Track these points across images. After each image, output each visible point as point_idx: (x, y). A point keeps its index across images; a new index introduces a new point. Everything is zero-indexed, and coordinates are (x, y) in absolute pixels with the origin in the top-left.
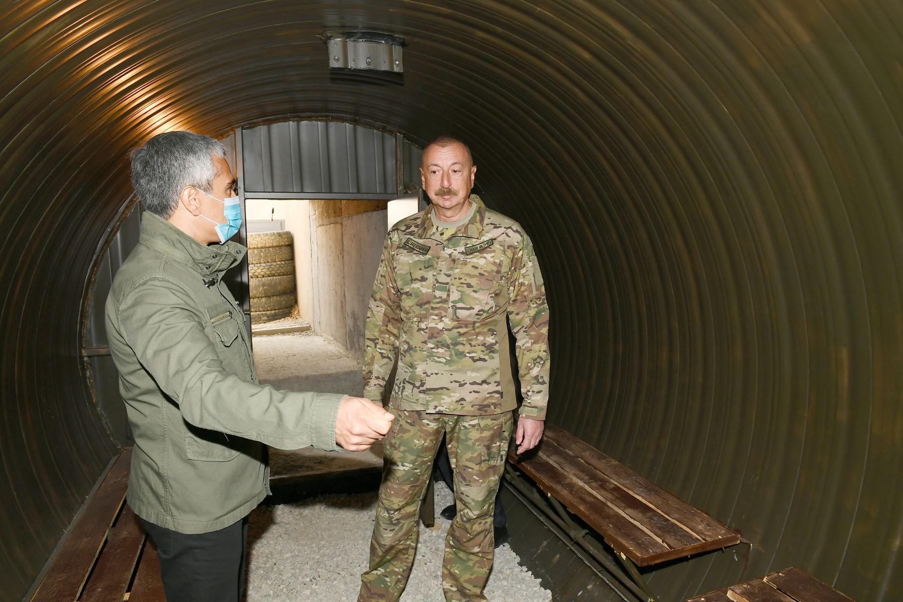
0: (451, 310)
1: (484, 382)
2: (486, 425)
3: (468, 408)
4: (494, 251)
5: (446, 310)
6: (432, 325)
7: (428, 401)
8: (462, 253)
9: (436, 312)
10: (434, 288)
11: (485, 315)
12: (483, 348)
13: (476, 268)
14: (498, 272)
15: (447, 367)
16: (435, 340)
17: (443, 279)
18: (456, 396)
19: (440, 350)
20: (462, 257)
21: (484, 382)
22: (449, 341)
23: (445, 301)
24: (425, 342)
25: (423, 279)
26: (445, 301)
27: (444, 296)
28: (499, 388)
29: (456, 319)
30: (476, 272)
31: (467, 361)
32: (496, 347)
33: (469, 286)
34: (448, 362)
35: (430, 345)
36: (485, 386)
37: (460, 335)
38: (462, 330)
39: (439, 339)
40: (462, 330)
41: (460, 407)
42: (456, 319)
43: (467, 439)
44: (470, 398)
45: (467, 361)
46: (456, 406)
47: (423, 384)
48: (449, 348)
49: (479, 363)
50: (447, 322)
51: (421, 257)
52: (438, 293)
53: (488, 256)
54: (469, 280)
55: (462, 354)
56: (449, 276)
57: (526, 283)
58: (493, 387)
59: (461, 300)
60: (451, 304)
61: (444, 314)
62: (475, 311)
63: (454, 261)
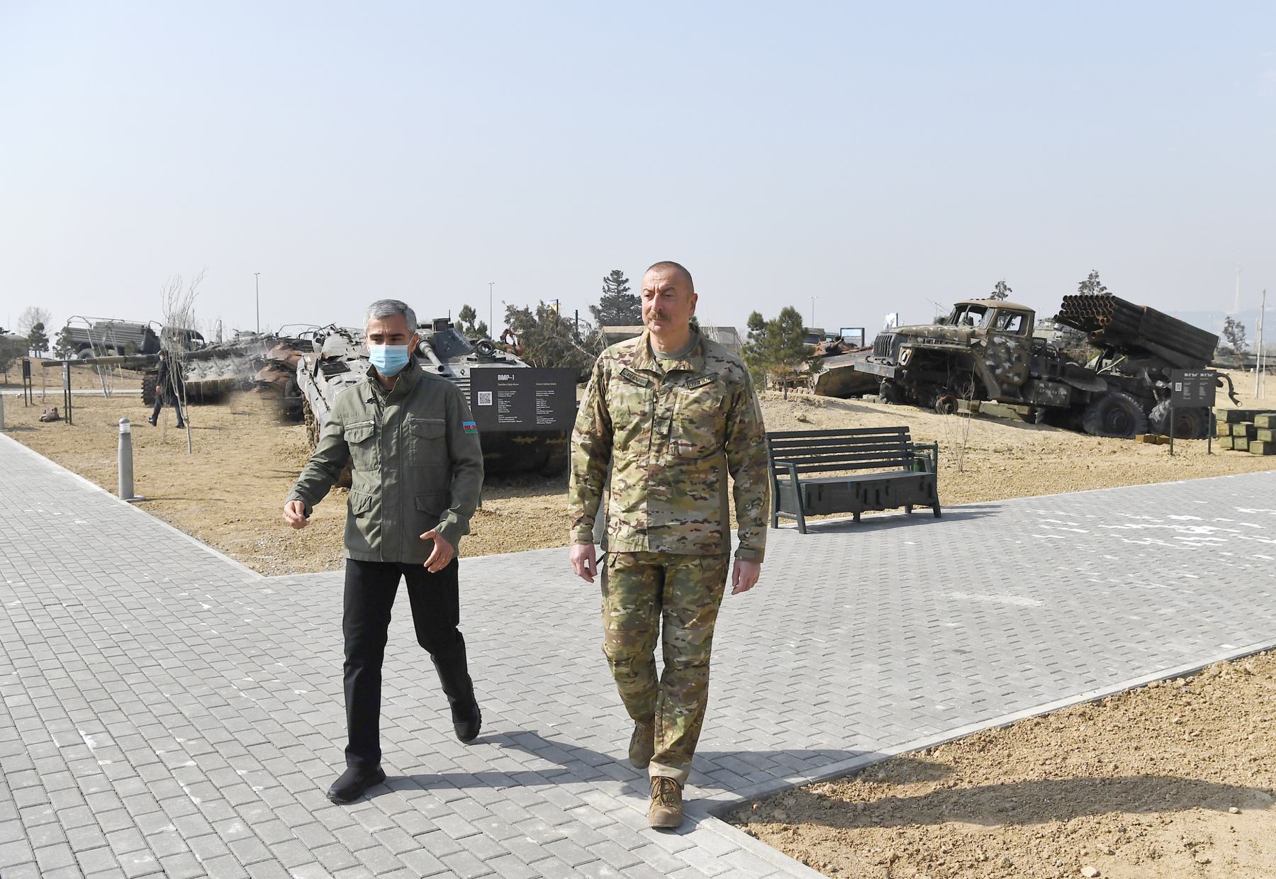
1: (705, 521)
2: (708, 565)
3: (690, 547)
6: (653, 462)
14: (720, 408)
15: (667, 506)
19: (661, 488)
21: (705, 521)
22: (671, 479)
28: (719, 528)
31: (688, 499)
32: (717, 485)
34: (669, 501)
37: (682, 471)
38: (684, 468)
40: (684, 468)
43: (689, 580)
44: (691, 536)
45: (688, 499)
48: (669, 484)
49: (700, 502)
55: (683, 493)
58: (714, 527)
62: (698, 448)
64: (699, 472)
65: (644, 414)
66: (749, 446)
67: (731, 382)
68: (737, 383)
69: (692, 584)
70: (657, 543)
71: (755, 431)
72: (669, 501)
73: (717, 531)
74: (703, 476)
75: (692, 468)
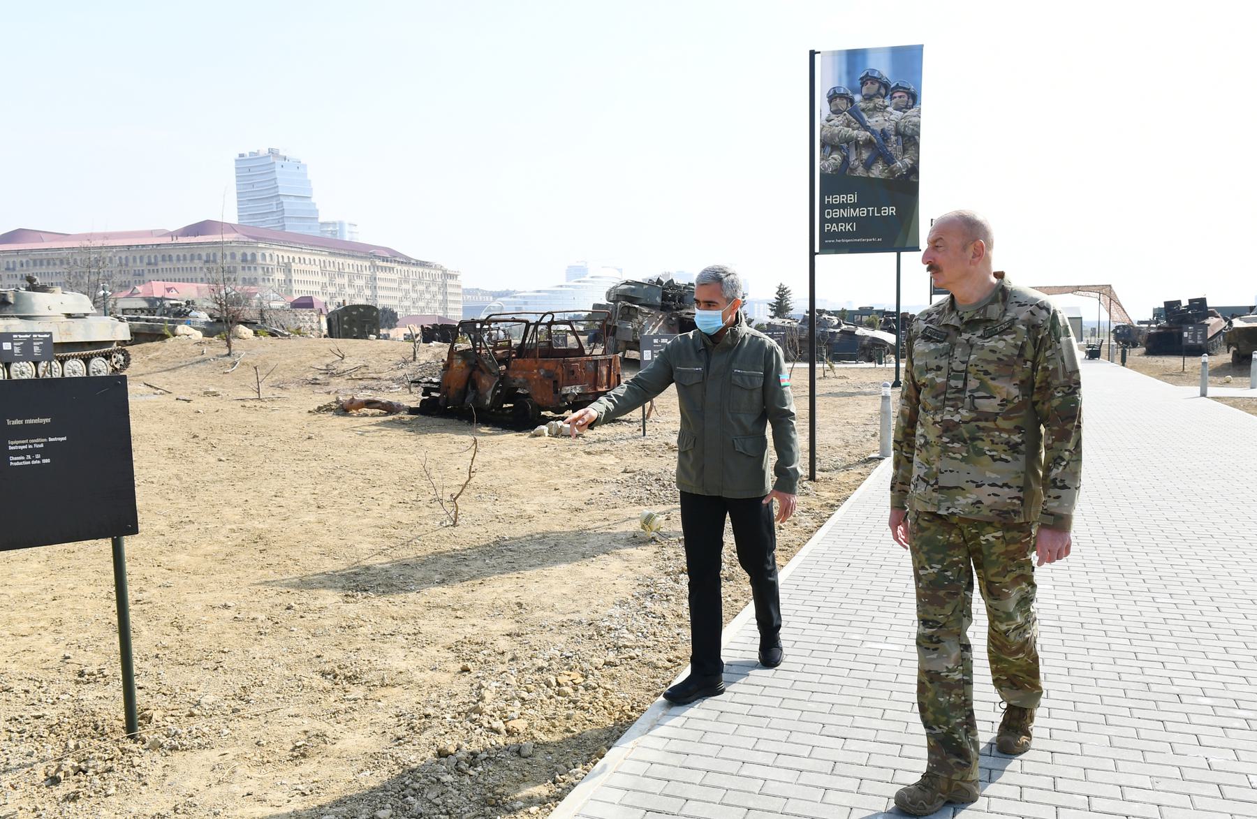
0: (968, 400)
1: (1005, 485)
3: (986, 512)
4: (1015, 332)
5: (963, 401)
6: (948, 417)
7: (940, 501)
8: (981, 337)
10: (948, 380)
11: (1010, 406)
12: (1006, 447)
13: (993, 351)
14: (1020, 355)
16: (949, 434)
17: (956, 365)
18: (972, 498)
19: (956, 445)
21: (1005, 485)
22: (966, 435)
23: (962, 390)
24: (940, 437)
26: (962, 390)
27: (960, 384)
28: (1021, 494)
29: (973, 408)
30: (994, 357)
32: (1022, 448)
33: (986, 373)
34: (964, 459)
35: (945, 439)
36: (1006, 489)
38: (982, 424)
39: (955, 432)
40: (982, 424)
41: (976, 510)
42: (973, 408)
44: (988, 501)
45: (986, 460)
46: (972, 509)
47: (936, 483)
48: (965, 441)
51: (940, 346)
52: (953, 383)
53: (1008, 338)
54: (987, 367)
55: (981, 453)
57: (1051, 367)
59: (977, 390)
60: (968, 394)
61: (960, 405)
63: (972, 346)
64: (1001, 430)
66: (1052, 397)
67: (1033, 326)
68: (1038, 326)
69: (994, 557)
70: (949, 504)
71: (1062, 379)
72: (964, 459)
73: (1018, 498)
74: (1005, 435)
75: (990, 425)
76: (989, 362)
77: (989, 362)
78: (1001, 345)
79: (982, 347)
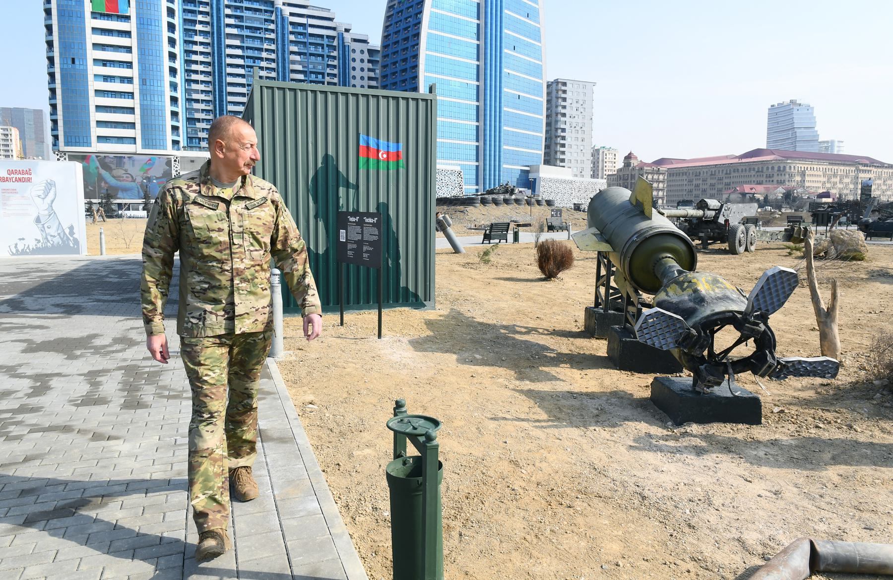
9: (237, 256)
19: (244, 285)
20: (246, 212)
22: (250, 277)
25: (220, 230)
29: (253, 259)
30: (260, 223)
33: (258, 233)
39: (243, 276)
42: (253, 259)
50: (247, 262)
56: (240, 227)
61: (243, 257)
65: (220, 230)
76: (259, 226)
77: (259, 226)
78: (262, 214)
79: (250, 216)
